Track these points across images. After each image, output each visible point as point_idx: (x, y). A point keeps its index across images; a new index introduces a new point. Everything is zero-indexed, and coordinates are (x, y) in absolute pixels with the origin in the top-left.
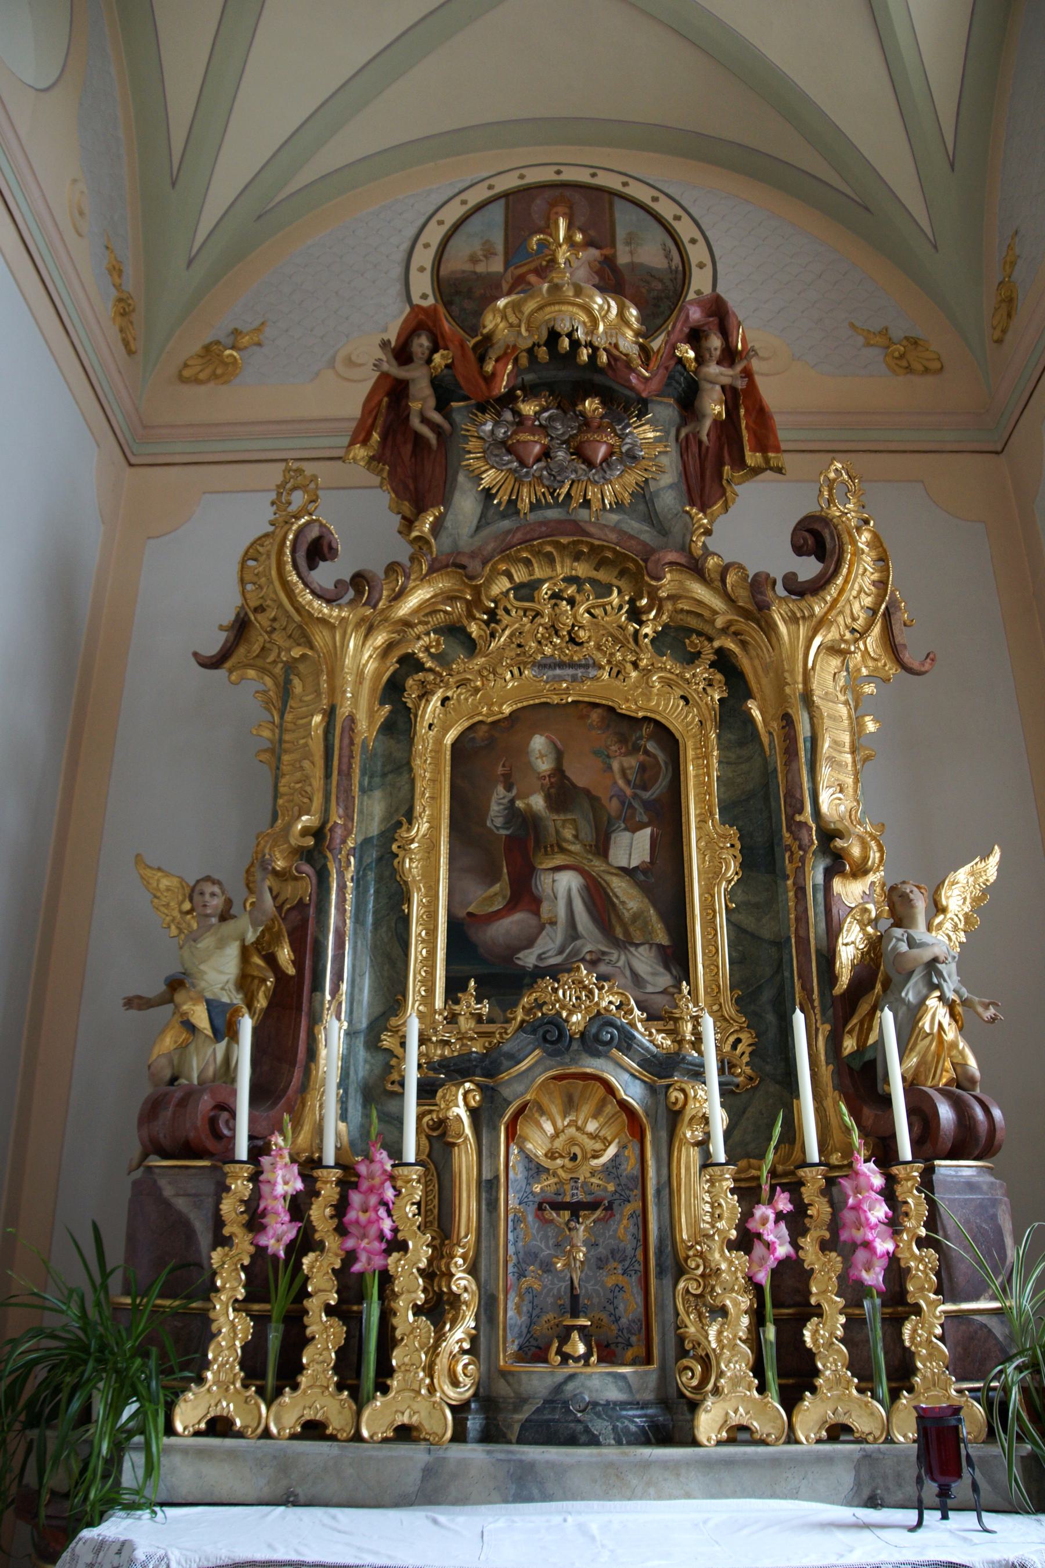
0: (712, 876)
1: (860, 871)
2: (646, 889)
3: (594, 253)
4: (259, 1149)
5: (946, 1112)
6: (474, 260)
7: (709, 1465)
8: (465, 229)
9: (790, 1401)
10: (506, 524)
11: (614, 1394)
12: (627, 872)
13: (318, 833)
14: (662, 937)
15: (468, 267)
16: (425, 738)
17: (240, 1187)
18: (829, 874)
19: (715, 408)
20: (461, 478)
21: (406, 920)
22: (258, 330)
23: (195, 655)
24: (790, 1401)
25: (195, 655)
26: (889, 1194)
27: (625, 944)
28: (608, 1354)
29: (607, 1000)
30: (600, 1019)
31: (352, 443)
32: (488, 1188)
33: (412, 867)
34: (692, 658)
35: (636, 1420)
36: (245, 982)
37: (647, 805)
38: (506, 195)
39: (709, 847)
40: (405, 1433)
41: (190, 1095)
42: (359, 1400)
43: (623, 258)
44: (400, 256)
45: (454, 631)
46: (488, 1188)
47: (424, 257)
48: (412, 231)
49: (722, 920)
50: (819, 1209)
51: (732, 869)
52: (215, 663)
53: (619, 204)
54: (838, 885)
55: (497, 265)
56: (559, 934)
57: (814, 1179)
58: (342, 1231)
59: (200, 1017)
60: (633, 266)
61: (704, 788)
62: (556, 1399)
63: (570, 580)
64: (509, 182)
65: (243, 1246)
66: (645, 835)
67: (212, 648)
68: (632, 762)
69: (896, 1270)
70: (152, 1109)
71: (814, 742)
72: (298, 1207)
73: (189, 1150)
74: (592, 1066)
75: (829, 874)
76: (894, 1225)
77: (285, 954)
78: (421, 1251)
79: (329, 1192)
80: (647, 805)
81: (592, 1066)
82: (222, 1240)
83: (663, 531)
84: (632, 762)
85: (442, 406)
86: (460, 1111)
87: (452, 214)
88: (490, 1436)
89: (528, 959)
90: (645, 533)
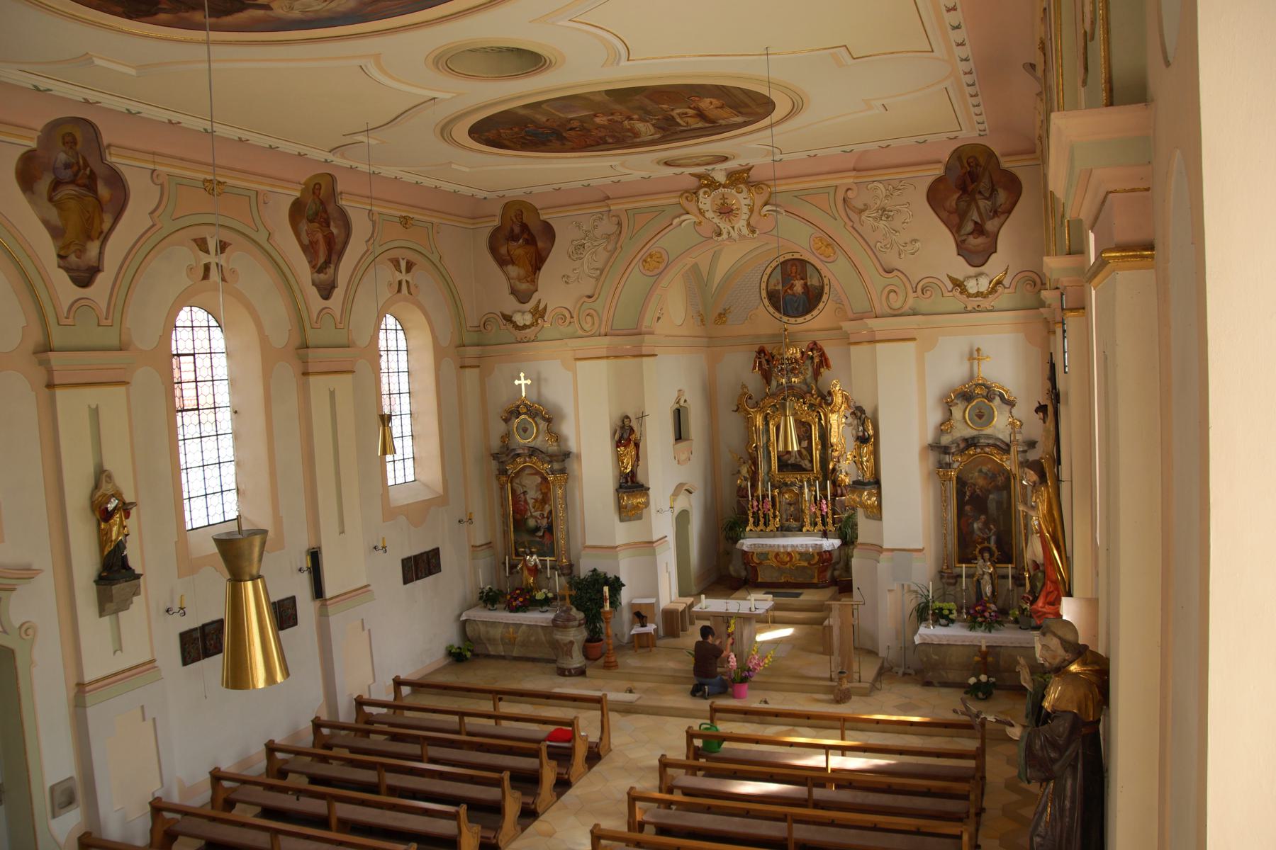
0: (816, 449)
1: (836, 450)
2: (807, 451)
3: (802, 282)
4: (752, 499)
5: (839, 491)
6: (775, 286)
7: (805, 534)
8: (773, 275)
9: (814, 527)
10: (781, 387)
11: (795, 526)
12: (804, 448)
13: (756, 446)
14: (809, 458)
15: (773, 288)
16: (771, 426)
17: (751, 503)
18: (832, 451)
19: (817, 360)
20: (773, 378)
21: (771, 457)
22: (729, 309)
23: (733, 411)
24: (814, 527)
25: (733, 411)
26: (827, 504)
27: (803, 459)
28: (795, 521)
29: (793, 480)
30: (792, 482)
31: (753, 370)
32: (780, 502)
33: (771, 449)
34: (813, 411)
35: (797, 529)
36: (748, 472)
37: (807, 437)
38: (781, 263)
39: (816, 444)
40: (772, 531)
41: (743, 489)
42: (766, 527)
43: (809, 284)
44: (758, 285)
45: (774, 405)
46: (780, 502)
47: (764, 285)
48: (760, 277)
49: (818, 455)
50: (819, 505)
51: (819, 447)
52: (736, 411)
53: (808, 264)
54: (833, 453)
55: (780, 287)
56: (794, 458)
57: (818, 502)
58: (763, 508)
59: (743, 478)
60: (812, 285)
61: (815, 434)
62: (788, 527)
63: (794, 396)
64: (782, 259)
65: (752, 510)
66: (806, 442)
67: (735, 409)
68: (804, 429)
69: (827, 513)
70: (738, 491)
71: (831, 429)
72: (758, 506)
73: (743, 497)
74: (791, 488)
75: (832, 451)
76: (827, 507)
77: (753, 468)
78: (772, 510)
79: (761, 503)
80: (807, 437)
81: (791, 488)
82: (749, 510)
83: (808, 387)
84: (804, 429)
85: (768, 364)
86: (776, 493)
87: (769, 271)
88: (782, 530)
89: (789, 462)
90: (804, 388)
